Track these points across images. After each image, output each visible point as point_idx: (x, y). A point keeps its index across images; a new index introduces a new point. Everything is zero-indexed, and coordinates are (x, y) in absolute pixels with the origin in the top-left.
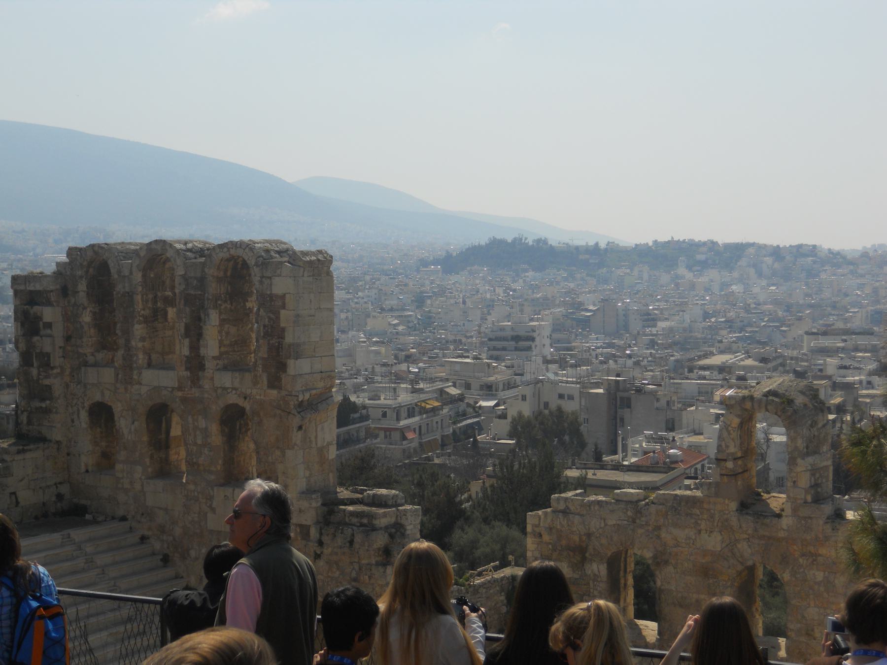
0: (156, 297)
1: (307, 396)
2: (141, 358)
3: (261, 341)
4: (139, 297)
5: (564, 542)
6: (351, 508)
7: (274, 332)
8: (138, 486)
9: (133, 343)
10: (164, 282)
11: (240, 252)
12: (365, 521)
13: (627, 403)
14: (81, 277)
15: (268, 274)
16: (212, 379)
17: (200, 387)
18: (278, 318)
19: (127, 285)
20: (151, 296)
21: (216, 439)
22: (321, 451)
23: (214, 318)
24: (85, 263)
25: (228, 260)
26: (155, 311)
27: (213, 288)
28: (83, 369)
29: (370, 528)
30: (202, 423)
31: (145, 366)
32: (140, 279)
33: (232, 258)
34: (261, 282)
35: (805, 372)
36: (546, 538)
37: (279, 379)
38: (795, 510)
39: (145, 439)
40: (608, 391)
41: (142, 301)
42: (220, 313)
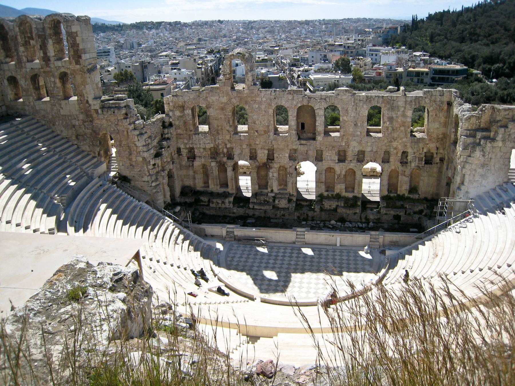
0: (25, 36)
1: (90, 66)
2: (25, 59)
5: (177, 105)
6: (111, 102)
7: (74, 45)
8: (32, 104)
9: (20, 54)
11: (57, 18)
12: (117, 105)
13: (146, 67)
15: (69, 25)
16: (54, 64)
17: (49, 67)
18: (76, 40)
21: (59, 84)
22: (97, 84)
23: (50, 42)
25: (52, 21)
26: (26, 42)
27: (48, 32)
29: (119, 108)
30: (53, 79)
33: (54, 20)
34: (67, 28)
36: (171, 104)
37: (80, 62)
38: (248, 88)
39: (31, 87)
40: (140, 64)
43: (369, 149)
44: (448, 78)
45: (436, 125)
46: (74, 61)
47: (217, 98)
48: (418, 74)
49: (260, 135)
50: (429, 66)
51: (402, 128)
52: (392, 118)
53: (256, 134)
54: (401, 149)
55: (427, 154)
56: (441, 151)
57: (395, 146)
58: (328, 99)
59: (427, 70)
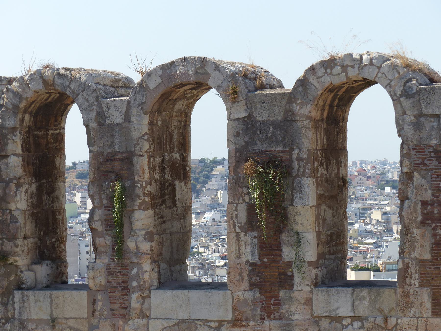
2: (147, 271)
3: (416, 232)
4: (145, 160)
10: (171, 136)
14: (14, 130)
16: (309, 302)
19: (116, 140)
20: (158, 160)
24: (22, 105)
28: (18, 294)
31: (156, 283)
32: (146, 129)
34: (417, 125)
35: (422, 305)
41: (149, 168)
42: (318, 185)
46: (425, 297)
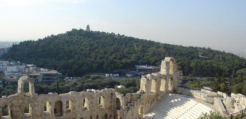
43: (84, 116)
44: (50, 78)
45: (108, 103)
47: (17, 101)
48: (35, 77)
49: (38, 117)
50: (40, 72)
51: (96, 106)
52: (92, 102)
53: (36, 117)
54: (96, 114)
55: (106, 115)
56: (110, 113)
57: (94, 114)
58: (68, 97)
59: (39, 74)
